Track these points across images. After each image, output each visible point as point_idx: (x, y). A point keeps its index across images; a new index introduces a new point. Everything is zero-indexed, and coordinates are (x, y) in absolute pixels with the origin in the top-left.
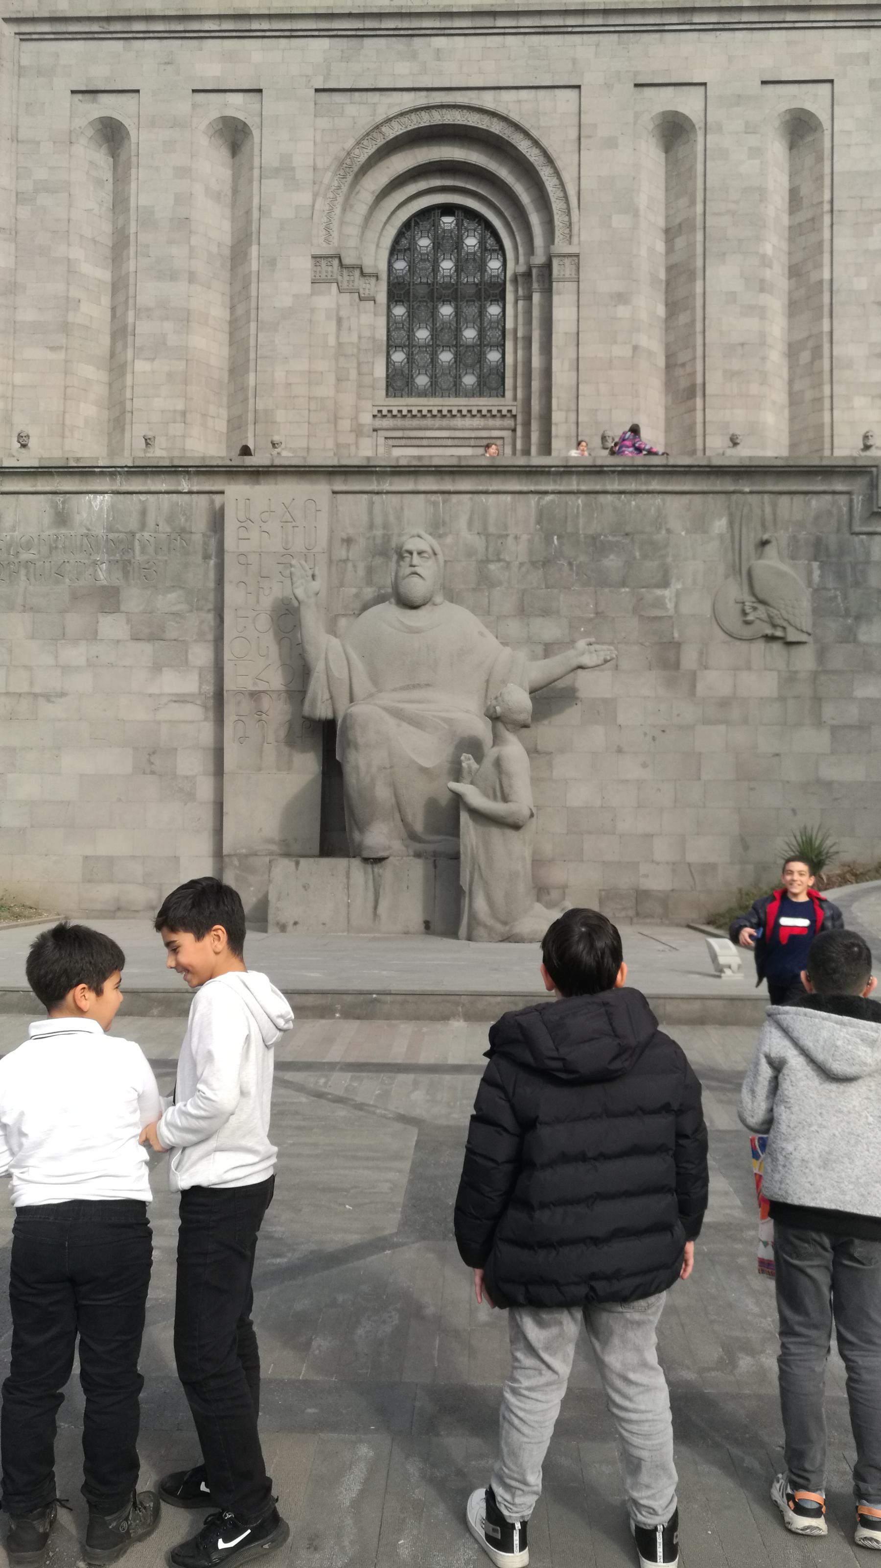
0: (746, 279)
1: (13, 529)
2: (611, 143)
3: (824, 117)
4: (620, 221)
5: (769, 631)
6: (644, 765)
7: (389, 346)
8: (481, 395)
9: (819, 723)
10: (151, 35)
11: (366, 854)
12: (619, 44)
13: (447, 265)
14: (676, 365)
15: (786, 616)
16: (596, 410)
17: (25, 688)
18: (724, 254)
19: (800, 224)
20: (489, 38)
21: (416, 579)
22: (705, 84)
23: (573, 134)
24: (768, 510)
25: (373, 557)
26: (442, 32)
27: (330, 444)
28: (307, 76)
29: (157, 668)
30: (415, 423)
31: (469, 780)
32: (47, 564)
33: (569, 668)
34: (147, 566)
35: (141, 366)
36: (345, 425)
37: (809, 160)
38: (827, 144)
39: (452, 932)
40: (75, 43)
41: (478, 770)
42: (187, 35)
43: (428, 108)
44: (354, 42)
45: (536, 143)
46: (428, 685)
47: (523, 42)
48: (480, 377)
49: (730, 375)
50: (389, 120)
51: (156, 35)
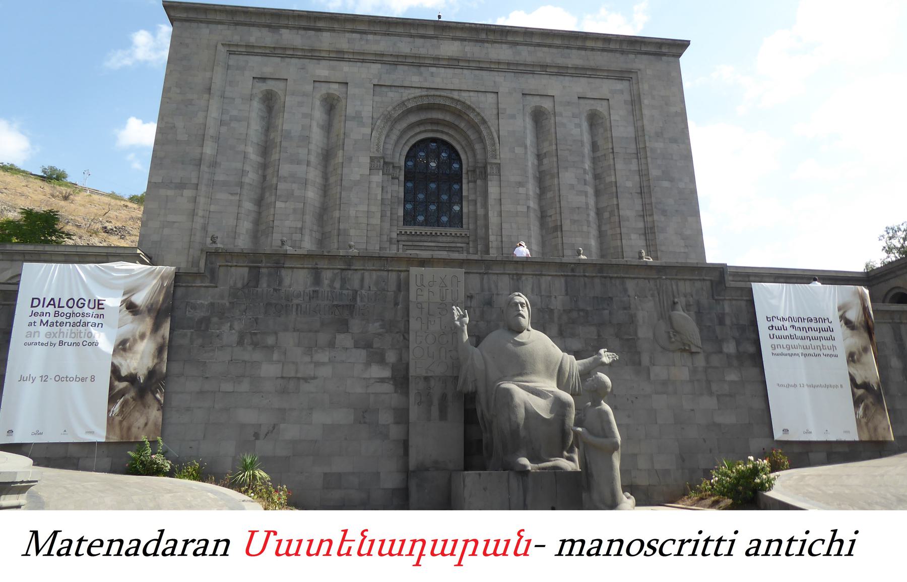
0: (578, 179)
1: (290, 286)
2: (513, 117)
3: (606, 113)
4: (519, 150)
6: (629, 416)
8: (450, 226)
9: (711, 394)
10: (295, 56)
12: (515, 77)
13: (433, 164)
14: (546, 216)
16: (511, 235)
17: (293, 374)
19: (598, 157)
20: (456, 70)
22: (554, 96)
23: (495, 112)
24: (674, 287)
26: (434, 65)
27: (378, 247)
28: (370, 79)
29: (368, 364)
30: (418, 238)
35: (279, 204)
36: (385, 238)
37: (601, 130)
38: (608, 125)
40: (257, 57)
42: (313, 58)
43: (427, 96)
44: (393, 67)
45: (478, 114)
47: (472, 73)
48: (450, 218)
49: (574, 222)
50: (409, 100)
51: (298, 56)
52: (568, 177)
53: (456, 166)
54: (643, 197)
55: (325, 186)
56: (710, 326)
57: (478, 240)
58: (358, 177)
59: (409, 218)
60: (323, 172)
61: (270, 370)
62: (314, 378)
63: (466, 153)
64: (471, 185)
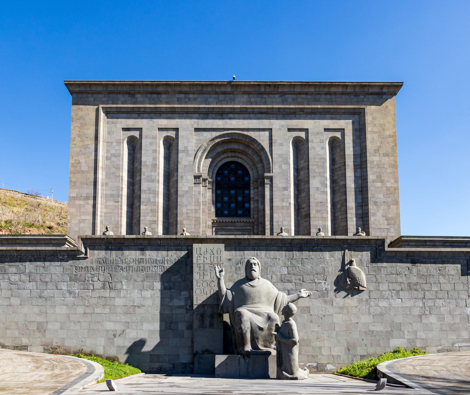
6: (319, 326)
7: (216, 202)
8: (244, 217)
13: (233, 179)
17: (132, 304)
18: (315, 176)
52: (314, 183)
53: (247, 179)
54: (363, 194)
55: (169, 195)
57: (259, 224)
58: (187, 189)
59: (219, 213)
60: (167, 186)
61: (119, 302)
62: (144, 306)
63: (252, 170)
64: (256, 190)
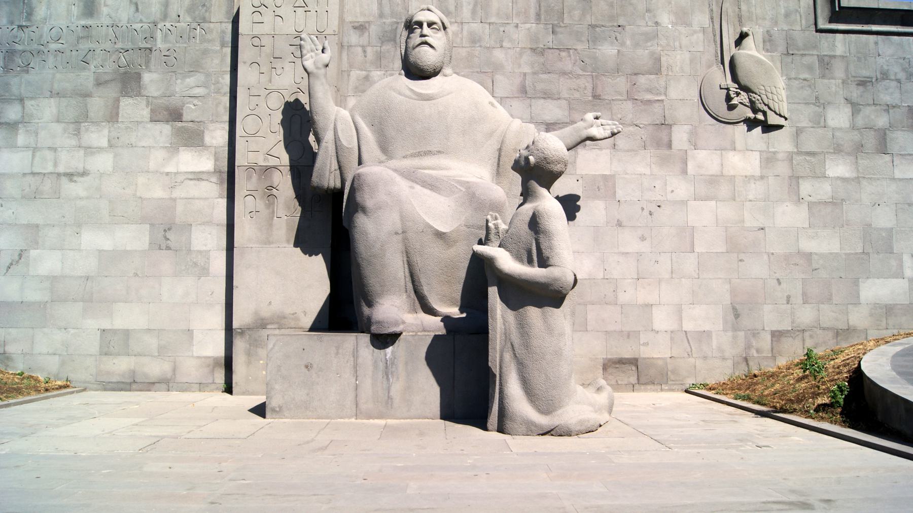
5: (752, 115)
6: (643, 238)
9: (799, 200)
11: (374, 329)
15: (767, 104)
17: (50, 168)
21: (426, 48)
25: (382, 43)
29: (173, 149)
31: (498, 243)
32: (74, 53)
33: (579, 140)
34: (167, 53)
39: (481, 422)
41: (507, 231)
46: (439, 152)
56: (805, 80)
